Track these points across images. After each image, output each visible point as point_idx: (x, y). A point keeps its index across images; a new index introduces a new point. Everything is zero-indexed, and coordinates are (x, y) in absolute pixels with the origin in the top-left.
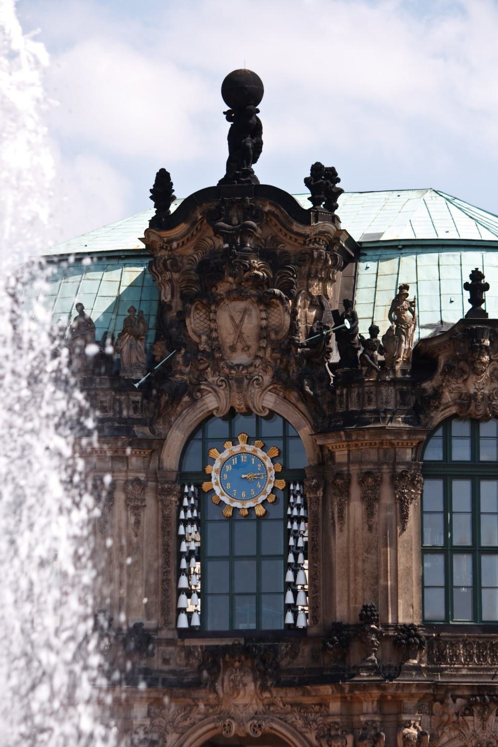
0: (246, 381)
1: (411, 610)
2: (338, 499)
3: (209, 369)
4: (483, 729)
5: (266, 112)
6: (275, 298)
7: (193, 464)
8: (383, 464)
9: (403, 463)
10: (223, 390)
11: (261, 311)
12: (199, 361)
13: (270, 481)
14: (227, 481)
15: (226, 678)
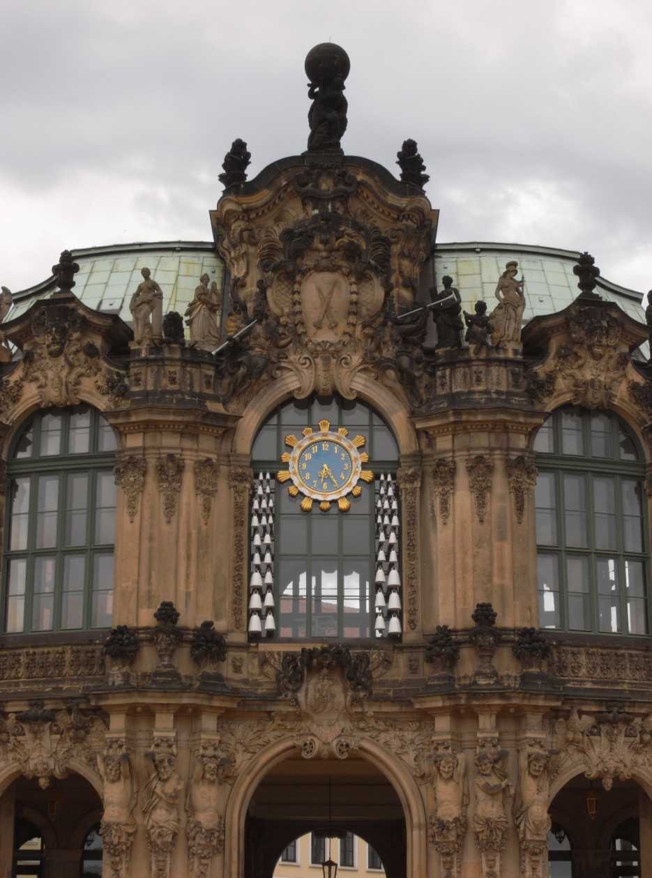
0: (334, 361)
1: (529, 613)
2: (440, 489)
3: (291, 345)
4: (611, 751)
5: (352, 89)
6: (369, 269)
7: (265, 451)
8: (492, 449)
9: (517, 450)
10: (307, 368)
11: (351, 284)
12: (280, 335)
13: (356, 472)
14: (305, 471)
15: (311, 687)
